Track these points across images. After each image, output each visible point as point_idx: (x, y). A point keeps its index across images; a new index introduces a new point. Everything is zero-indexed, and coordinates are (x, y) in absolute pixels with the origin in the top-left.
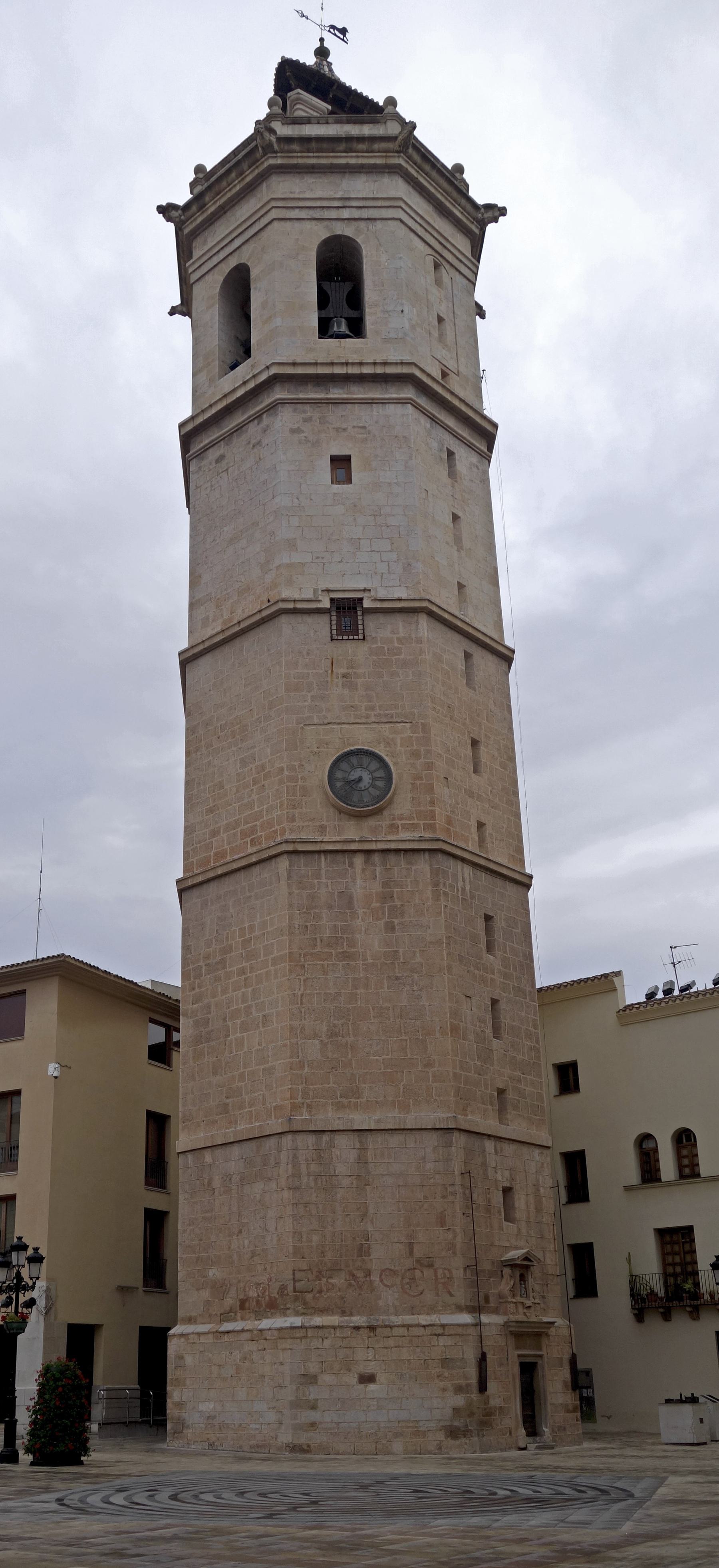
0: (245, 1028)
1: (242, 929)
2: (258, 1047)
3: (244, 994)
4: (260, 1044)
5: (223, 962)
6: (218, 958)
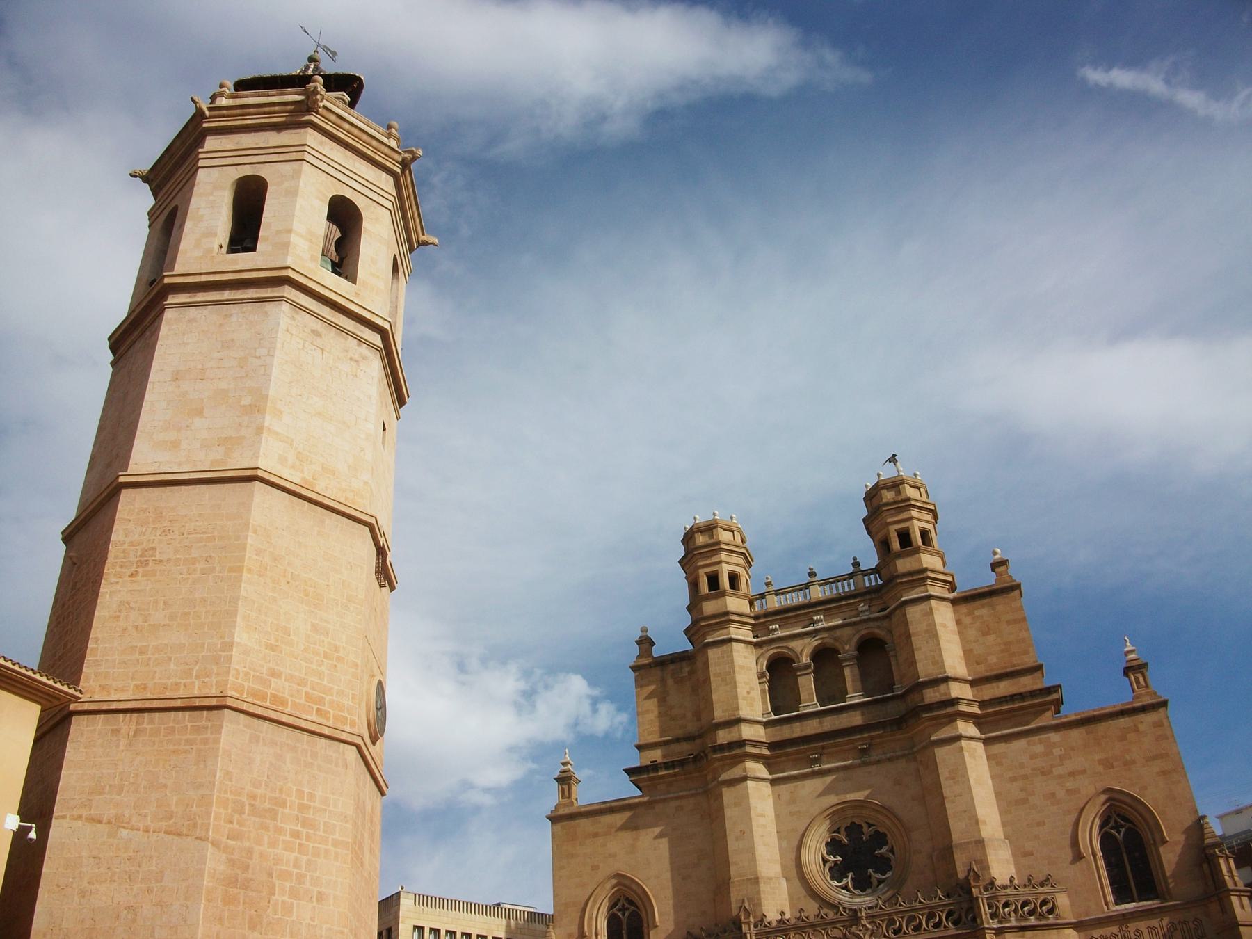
0: (294, 894)
1: (300, 793)
2: (308, 921)
3: (296, 859)
4: (312, 919)
5: (273, 814)
6: (267, 805)
